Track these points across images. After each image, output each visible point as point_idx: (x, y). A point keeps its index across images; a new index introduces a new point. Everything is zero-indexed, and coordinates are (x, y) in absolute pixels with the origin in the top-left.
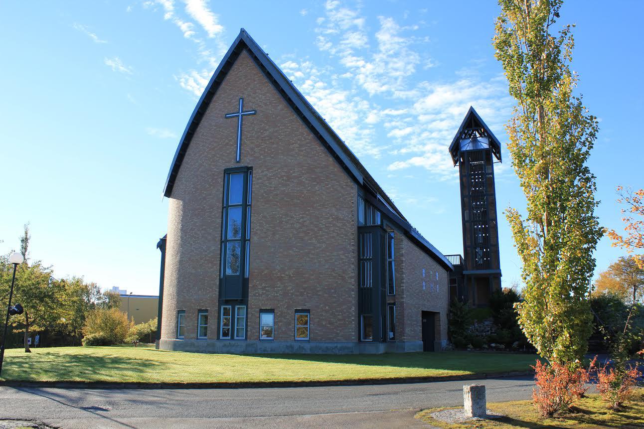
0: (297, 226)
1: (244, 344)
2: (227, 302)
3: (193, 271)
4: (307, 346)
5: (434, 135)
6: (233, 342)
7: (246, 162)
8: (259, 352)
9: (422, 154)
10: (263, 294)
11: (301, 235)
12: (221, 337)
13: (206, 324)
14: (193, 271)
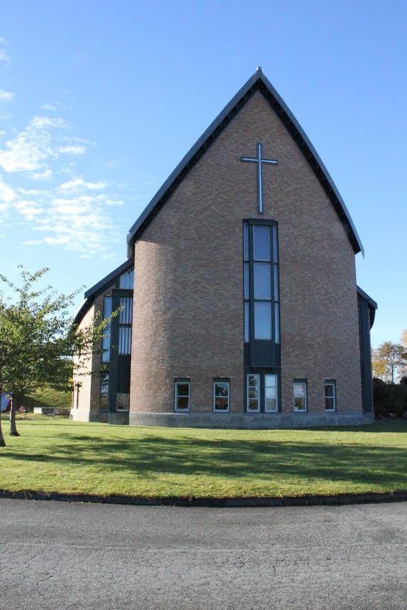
0: (323, 292)
1: (279, 417)
2: (253, 371)
3: (203, 332)
4: (336, 418)
5: (63, 218)
6: (265, 416)
7: (271, 214)
8: (295, 425)
9: (52, 234)
10: (297, 362)
11: (327, 302)
12: (248, 410)
13: (327, 399)
14: (203, 332)
